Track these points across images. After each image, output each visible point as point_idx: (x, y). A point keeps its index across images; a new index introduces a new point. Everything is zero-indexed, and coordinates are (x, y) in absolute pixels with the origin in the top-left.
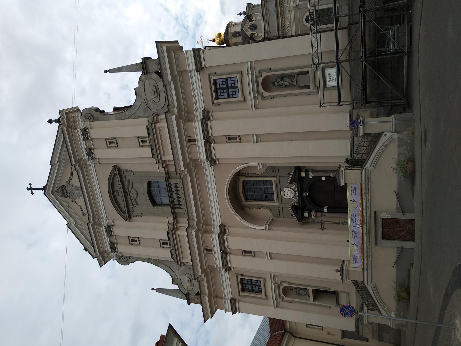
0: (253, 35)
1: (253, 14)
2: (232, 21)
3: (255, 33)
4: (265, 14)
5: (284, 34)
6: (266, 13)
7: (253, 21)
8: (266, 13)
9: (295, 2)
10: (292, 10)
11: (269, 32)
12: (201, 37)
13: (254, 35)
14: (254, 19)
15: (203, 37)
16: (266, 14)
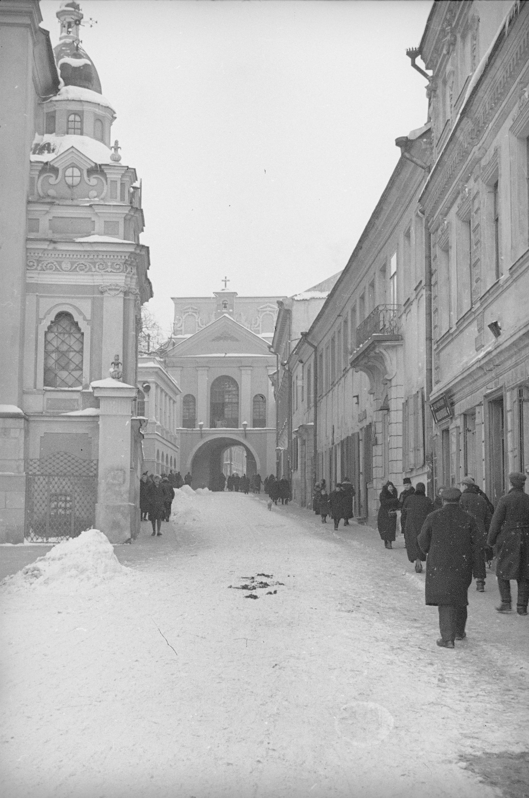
0: (53, 173)
1: (104, 182)
2: (116, 118)
3: (58, 181)
4: (96, 211)
5: (40, 255)
6: (99, 214)
7: (89, 180)
8: (99, 214)
9: (109, 289)
10: (95, 281)
11: (54, 217)
12: (91, 22)
13: (51, 175)
14: (93, 181)
15: (91, 26)
16: (96, 214)
